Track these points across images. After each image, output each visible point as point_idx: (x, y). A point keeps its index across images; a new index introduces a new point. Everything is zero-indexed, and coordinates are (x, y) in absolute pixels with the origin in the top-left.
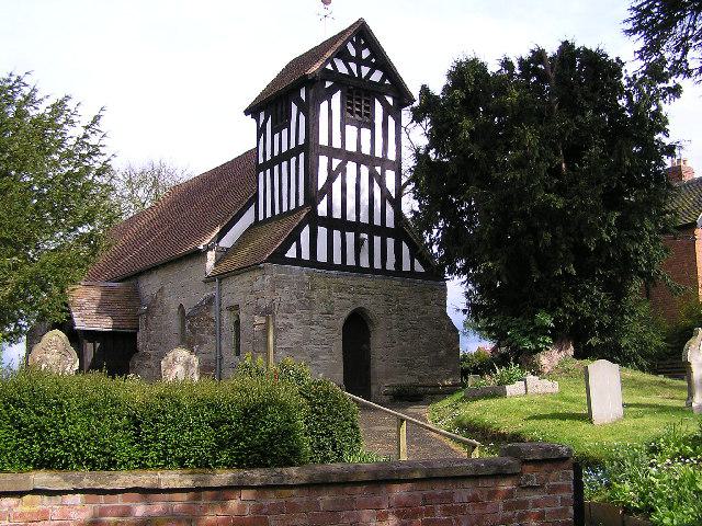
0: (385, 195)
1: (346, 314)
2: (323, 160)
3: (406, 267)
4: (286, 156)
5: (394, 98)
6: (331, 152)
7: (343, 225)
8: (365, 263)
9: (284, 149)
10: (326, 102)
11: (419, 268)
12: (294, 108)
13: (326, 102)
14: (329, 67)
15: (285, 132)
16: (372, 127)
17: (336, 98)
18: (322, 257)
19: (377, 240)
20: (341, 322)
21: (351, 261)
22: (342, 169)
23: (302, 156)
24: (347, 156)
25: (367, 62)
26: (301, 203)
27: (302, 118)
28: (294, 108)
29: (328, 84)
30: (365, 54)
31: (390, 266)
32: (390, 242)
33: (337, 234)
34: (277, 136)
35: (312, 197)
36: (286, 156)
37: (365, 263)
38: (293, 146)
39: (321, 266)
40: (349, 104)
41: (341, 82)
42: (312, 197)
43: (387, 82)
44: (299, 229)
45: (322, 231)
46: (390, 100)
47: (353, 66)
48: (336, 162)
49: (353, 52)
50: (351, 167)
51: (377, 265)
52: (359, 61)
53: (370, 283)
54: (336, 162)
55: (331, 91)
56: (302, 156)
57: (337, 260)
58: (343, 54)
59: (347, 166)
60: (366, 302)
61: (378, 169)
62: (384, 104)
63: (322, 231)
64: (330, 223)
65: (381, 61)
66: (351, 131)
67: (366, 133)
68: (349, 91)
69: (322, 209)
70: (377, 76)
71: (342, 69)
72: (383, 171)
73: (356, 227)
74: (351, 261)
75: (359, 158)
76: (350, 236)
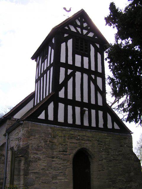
0: (97, 88)
1: (74, 152)
2: (62, 70)
3: (110, 126)
6: (66, 66)
7: (74, 103)
8: (86, 123)
11: (116, 127)
12: (50, 48)
14: (67, 28)
15: (46, 60)
16: (89, 56)
17: (70, 42)
20: (71, 156)
21: (78, 122)
22: (73, 75)
24: (75, 69)
25: (86, 28)
27: (53, 51)
29: (66, 35)
31: (101, 125)
32: (101, 113)
33: (70, 108)
34: (43, 64)
39: (60, 124)
41: (72, 35)
45: (61, 106)
46: (98, 46)
47: (79, 29)
48: (70, 71)
49: (79, 23)
50: (78, 74)
51: (94, 125)
57: (70, 121)
60: (88, 145)
61: (93, 76)
62: (95, 47)
63: (61, 106)
64: (66, 101)
66: (78, 58)
67: (86, 59)
70: (91, 35)
71: (73, 29)
73: (81, 104)
74: (78, 122)
75: (82, 70)
76: (78, 109)
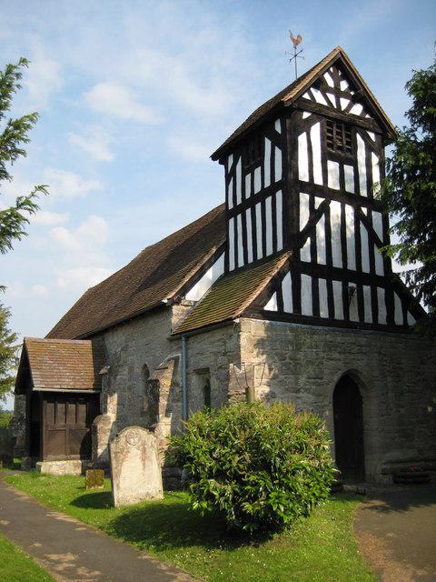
0: (372, 235)
1: (336, 378)
2: (304, 198)
3: (399, 320)
4: (259, 198)
5: (376, 134)
6: (312, 189)
7: (328, 272)
8: (354, 317)
9: (258, 189)
10: (305, 134)
11: (411, 321)
12: (268, 143)
13: (305, 134)
14: (306, 96)
15: (258, 171)
16: (354, 163)
17: (316, 130)
18: (307, 309)
19: (367, 289)
20: (331, 387)
21: (339, 314)
22: (325, 209)
23: (279, 195)
24: (329, 195)
25: (345, 95)
26: (280, 247)
27: (278, 153)
28: (268, 143)
29: (306, 115)
30: (344, 86)
31: (382, 319)
32: (381, 292)
33: (322, 282)
34: (248, 177)
35: (294, 238)
36: (259, 198)
37: (354, 317)
38: (267, 184)
39: (305, 320)
40: (329, 138)
41: (318, 112)
42: (294, 238)
43: (367, 116)
44: (281, 276)
45: (306, 280)
46: (372, 136)
47: (332, 98)
48: (319, 201)
49: (330, 82)
50: (335, 207)
51: (368, 318)
52: (338, 93)
53: (362, 340)
54: (319, 201)
55: (309, 123)
56: (279, 195)
57: (324, 314)
58: (319, 84)
59: (330, 205)
60: (360, 364)
61: (364, 210)
62: (366, 138)
63: (306, 280)
64: (314, 269)
65: (360, 94)
66: (333, 166)
67: (349, 170)
68: (329, 124)
69: (305, 256)
70: (357, 110)
71: (319, 97)
72: (369, 213)
73: (343, 274)
74: (339, 314)
75: (344, 197)
76: (337, 285)
